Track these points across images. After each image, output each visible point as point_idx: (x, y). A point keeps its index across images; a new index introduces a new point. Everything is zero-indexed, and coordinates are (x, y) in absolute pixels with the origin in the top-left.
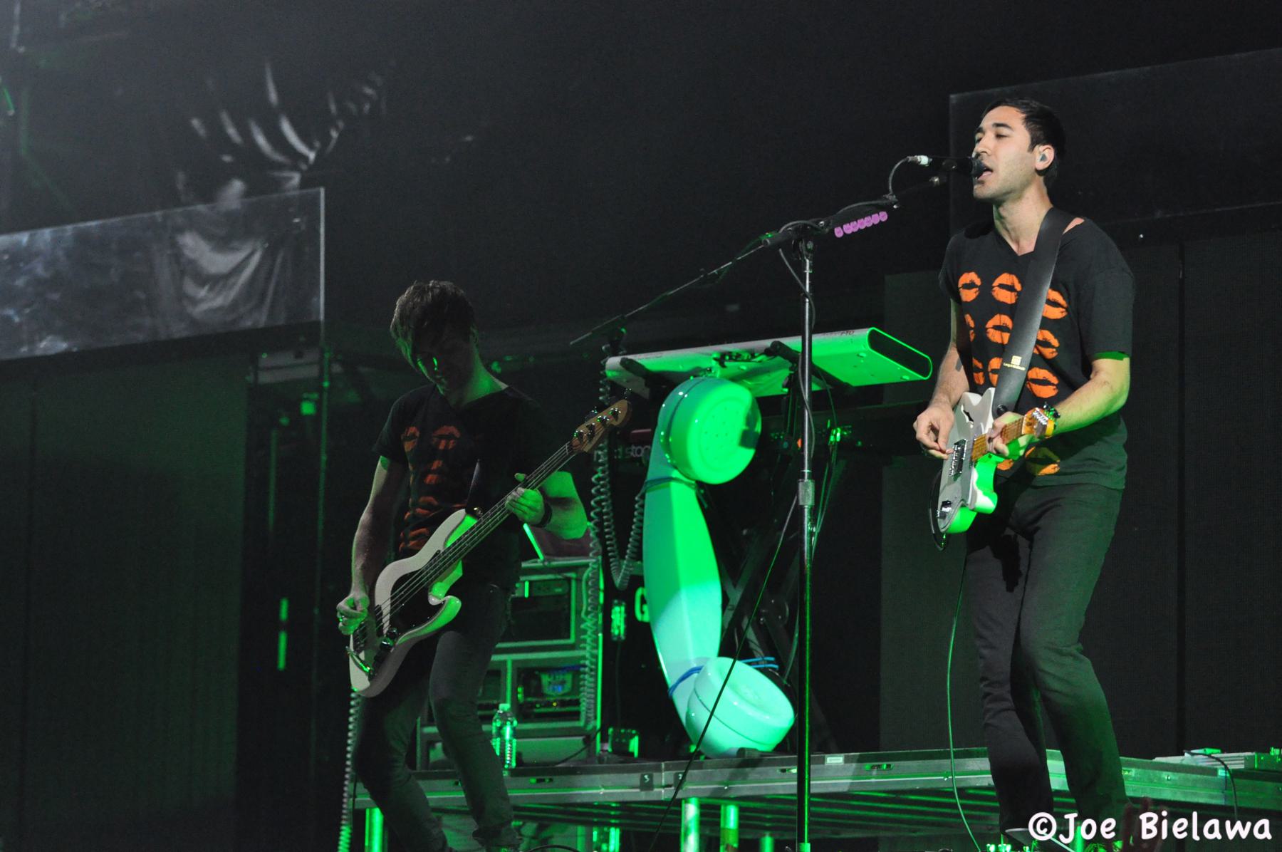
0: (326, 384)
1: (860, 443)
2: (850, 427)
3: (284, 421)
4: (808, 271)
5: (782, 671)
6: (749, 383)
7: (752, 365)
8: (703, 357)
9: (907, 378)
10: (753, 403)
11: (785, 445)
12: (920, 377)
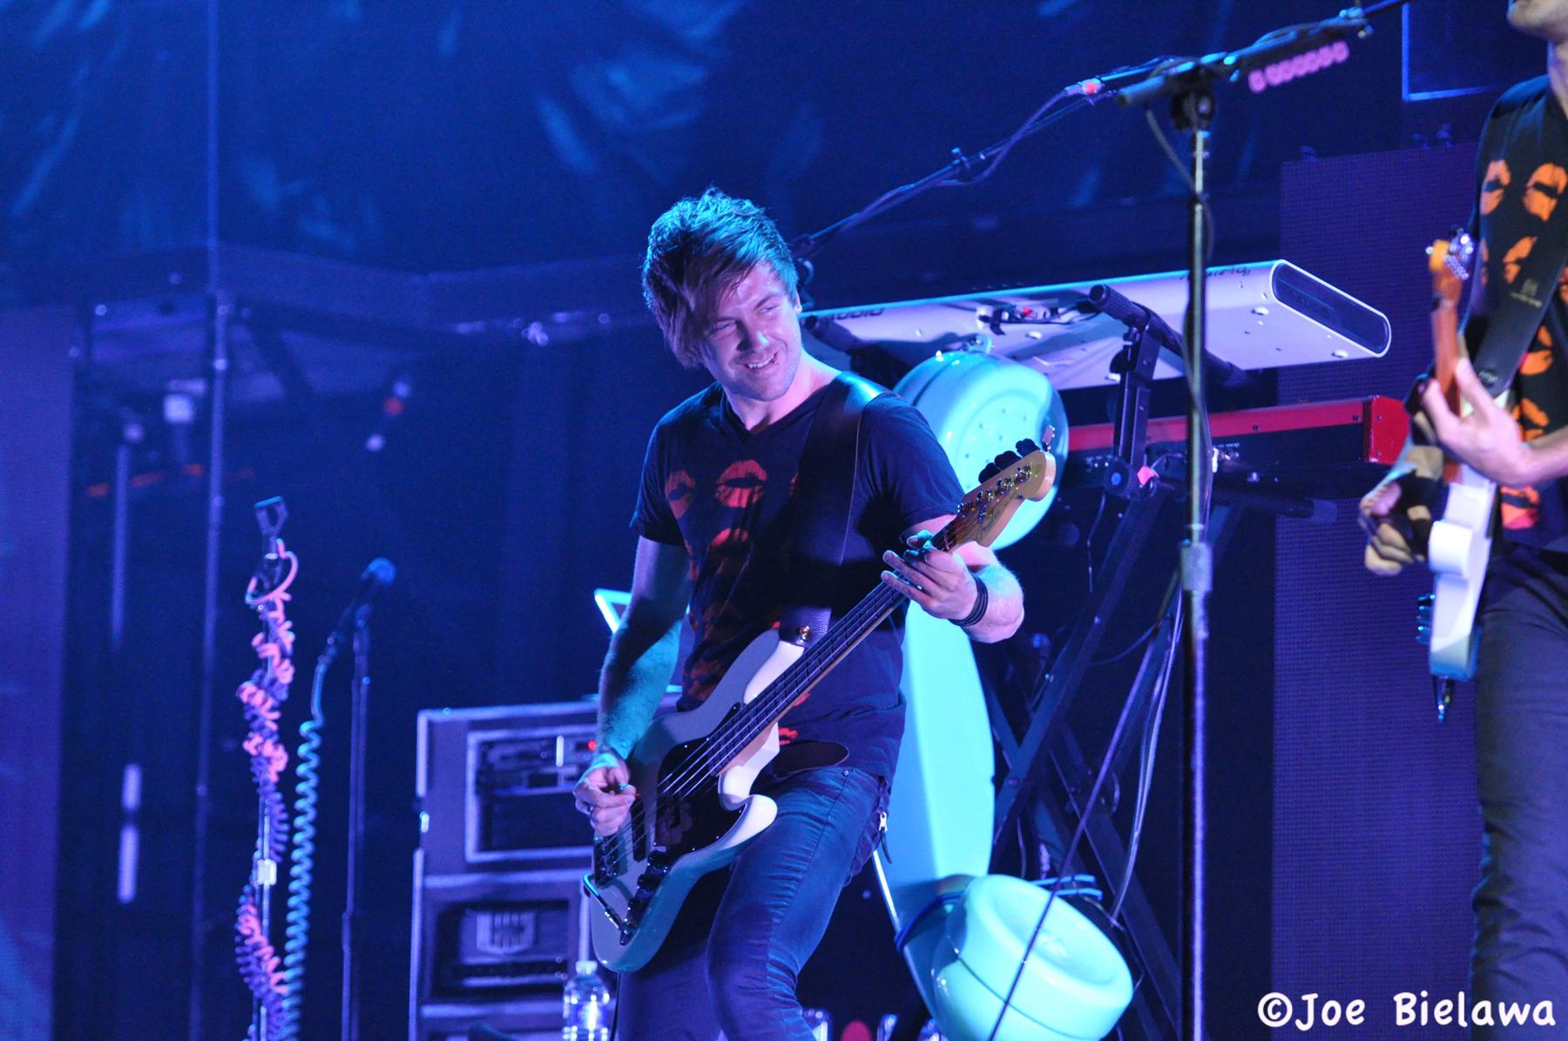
0: (220, 364)
1: (1255, 476)
2: (1236, 445)
3: (134, 433)
4: (1200, 154)
5: (1108, 901)
6: (1045, 363)
7: (1053, 329)
8: (968, 320)
9: (1344, 354)
10: (1053, 401)
11: (1116, 478)
12: (1370, 354)
